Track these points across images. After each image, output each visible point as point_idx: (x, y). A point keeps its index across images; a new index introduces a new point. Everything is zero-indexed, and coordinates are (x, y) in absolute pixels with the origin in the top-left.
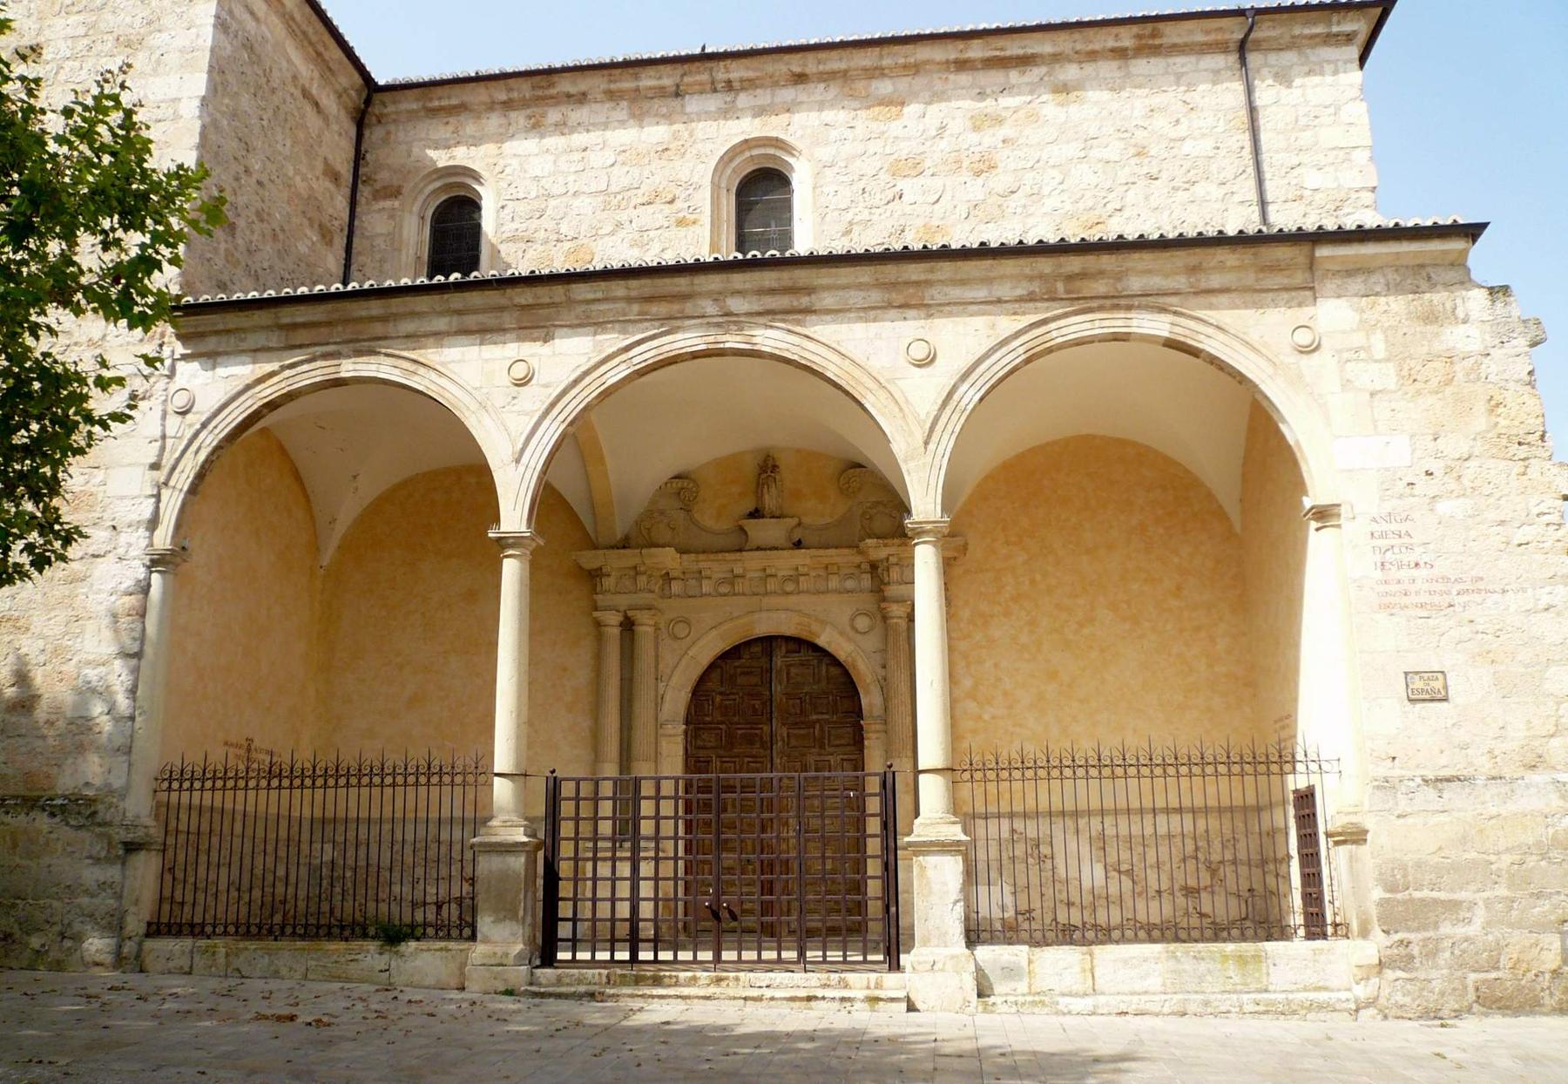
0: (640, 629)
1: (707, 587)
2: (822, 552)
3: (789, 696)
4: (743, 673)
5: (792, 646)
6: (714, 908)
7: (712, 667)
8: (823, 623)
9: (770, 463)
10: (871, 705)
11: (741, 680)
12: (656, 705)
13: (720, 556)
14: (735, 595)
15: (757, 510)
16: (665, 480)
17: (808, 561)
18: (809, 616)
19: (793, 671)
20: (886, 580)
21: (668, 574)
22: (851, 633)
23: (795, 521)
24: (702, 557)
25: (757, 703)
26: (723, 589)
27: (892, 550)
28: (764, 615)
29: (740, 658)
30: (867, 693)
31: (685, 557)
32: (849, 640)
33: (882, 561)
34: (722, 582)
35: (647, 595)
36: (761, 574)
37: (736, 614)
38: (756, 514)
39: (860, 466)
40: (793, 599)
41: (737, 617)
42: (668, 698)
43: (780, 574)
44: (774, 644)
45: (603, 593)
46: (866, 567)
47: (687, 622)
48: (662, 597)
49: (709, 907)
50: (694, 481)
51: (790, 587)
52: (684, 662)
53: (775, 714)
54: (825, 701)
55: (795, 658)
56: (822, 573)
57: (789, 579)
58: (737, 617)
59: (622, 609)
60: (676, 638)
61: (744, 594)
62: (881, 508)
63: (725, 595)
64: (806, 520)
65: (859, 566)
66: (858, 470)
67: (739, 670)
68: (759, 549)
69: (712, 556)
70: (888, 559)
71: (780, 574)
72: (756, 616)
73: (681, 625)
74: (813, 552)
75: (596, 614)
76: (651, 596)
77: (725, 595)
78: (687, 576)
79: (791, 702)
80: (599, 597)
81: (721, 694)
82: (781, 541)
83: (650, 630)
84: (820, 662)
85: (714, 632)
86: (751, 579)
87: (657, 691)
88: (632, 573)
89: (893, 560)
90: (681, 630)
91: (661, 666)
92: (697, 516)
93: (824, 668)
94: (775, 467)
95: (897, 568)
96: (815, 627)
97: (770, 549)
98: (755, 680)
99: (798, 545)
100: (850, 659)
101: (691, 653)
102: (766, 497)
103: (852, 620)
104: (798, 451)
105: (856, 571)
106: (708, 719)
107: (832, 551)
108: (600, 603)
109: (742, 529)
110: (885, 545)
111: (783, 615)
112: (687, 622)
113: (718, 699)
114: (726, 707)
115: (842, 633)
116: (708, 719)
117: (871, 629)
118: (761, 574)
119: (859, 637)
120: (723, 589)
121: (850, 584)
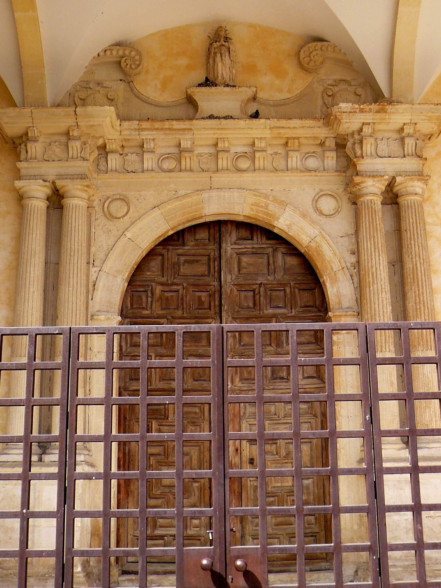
0: (70, 203)
1: (149, 161)
2: (283, 123)
3: (240, 287)
4: (186, 261)
5: (244, 233)
6: (218, 568)
7: (151, 254)
8: (283, 204)
9: (222, 33)
10: (339, 296)
11: (183, 270)
12: (88, 292)
13: (167, 124)
14: (181, 171)
15: (207, 79)
16: (105, 46)
17: (267, 134)
18: (266, 197)
19: (245, 259)
20: (359, 153)
21: (104, 146)
22: (315, 216)
23: (249, 92)
24: (145, 125)
25: (204, 296)
26: (166, 165)
27: (368, 118)
28: (214, 193)
29: (184, 245)
30: (335, 281)
31: (126, 124)
32: (313, 222)
33: (353, 134)
34: (168, 157)
35: (80, 163)
36: (212, 150)
37: (182, 192)
38: (208, 83)
39: (320, 40)
40: (247, 178)
41: (185, 196)
42: (100, 285)
43: (233, 150)
44: (223, 229)
45: (26, 160)
46: (331, 143)
47: (124, 200)
48: (99, 171)
49: (210, 569)
50: (137, 51)
51: (244, 164)
52: (120, 243)
53: (225, 308)
54: (282, 294)
55: (248, 245)
56: (281, 150)
57: (244, 155)
58: (185, 196)
59: (51, 178)
60: (111, 217)
61: (191, 170)
62: (343, 86)
63: (170, 171)
64: (260, 95)
65: (322, 144)
66: (320, 44)
67: (182, 259)
68: (211, 117)
69: (157, 125)
70: (361, 130)
71: (233, 150)
72: (205, 195)
73: (118, 203)
74: (273, 122)
75: (18, 184)
76: (85, 164)
77: (170, 171)
78: (126, 150)
79: (243, 294)
80: (20, 165)
81: (162, 284)
82: (236, 113)
83: (83, 204)
84: (275, 250)
85: (157, 212)
86: (200, 155)
87: (88, 276)
88: (64, 139)
89: (367, 130)
90: (119, 209)
91: (93, 249)
92: (139, 87)
93: (280, 256)
94: (227, 39)
95: (372, 140)
96: (273, 208)
97: (226, 118)
98: (202, 269)
99: (256, 115)
100: (313, 244)
101: (129, 235)
102: (220, 65)
103: (315, 201)
104: (251, 26)
105: (319, 150)
106: (145, 312)
107: (295, 123)
108: (23, 172)
109: (191, 101)
110: (362, 111)
111: (236, 194)
112: (124, 200)
113: (158, 290)
114: (167, 299)
115: (304, 216)
116: (145, 312)
117: (337, 211)
118: (212, 150)
119: (323, 220)
120: (167, 165)
121: (312, 163)
